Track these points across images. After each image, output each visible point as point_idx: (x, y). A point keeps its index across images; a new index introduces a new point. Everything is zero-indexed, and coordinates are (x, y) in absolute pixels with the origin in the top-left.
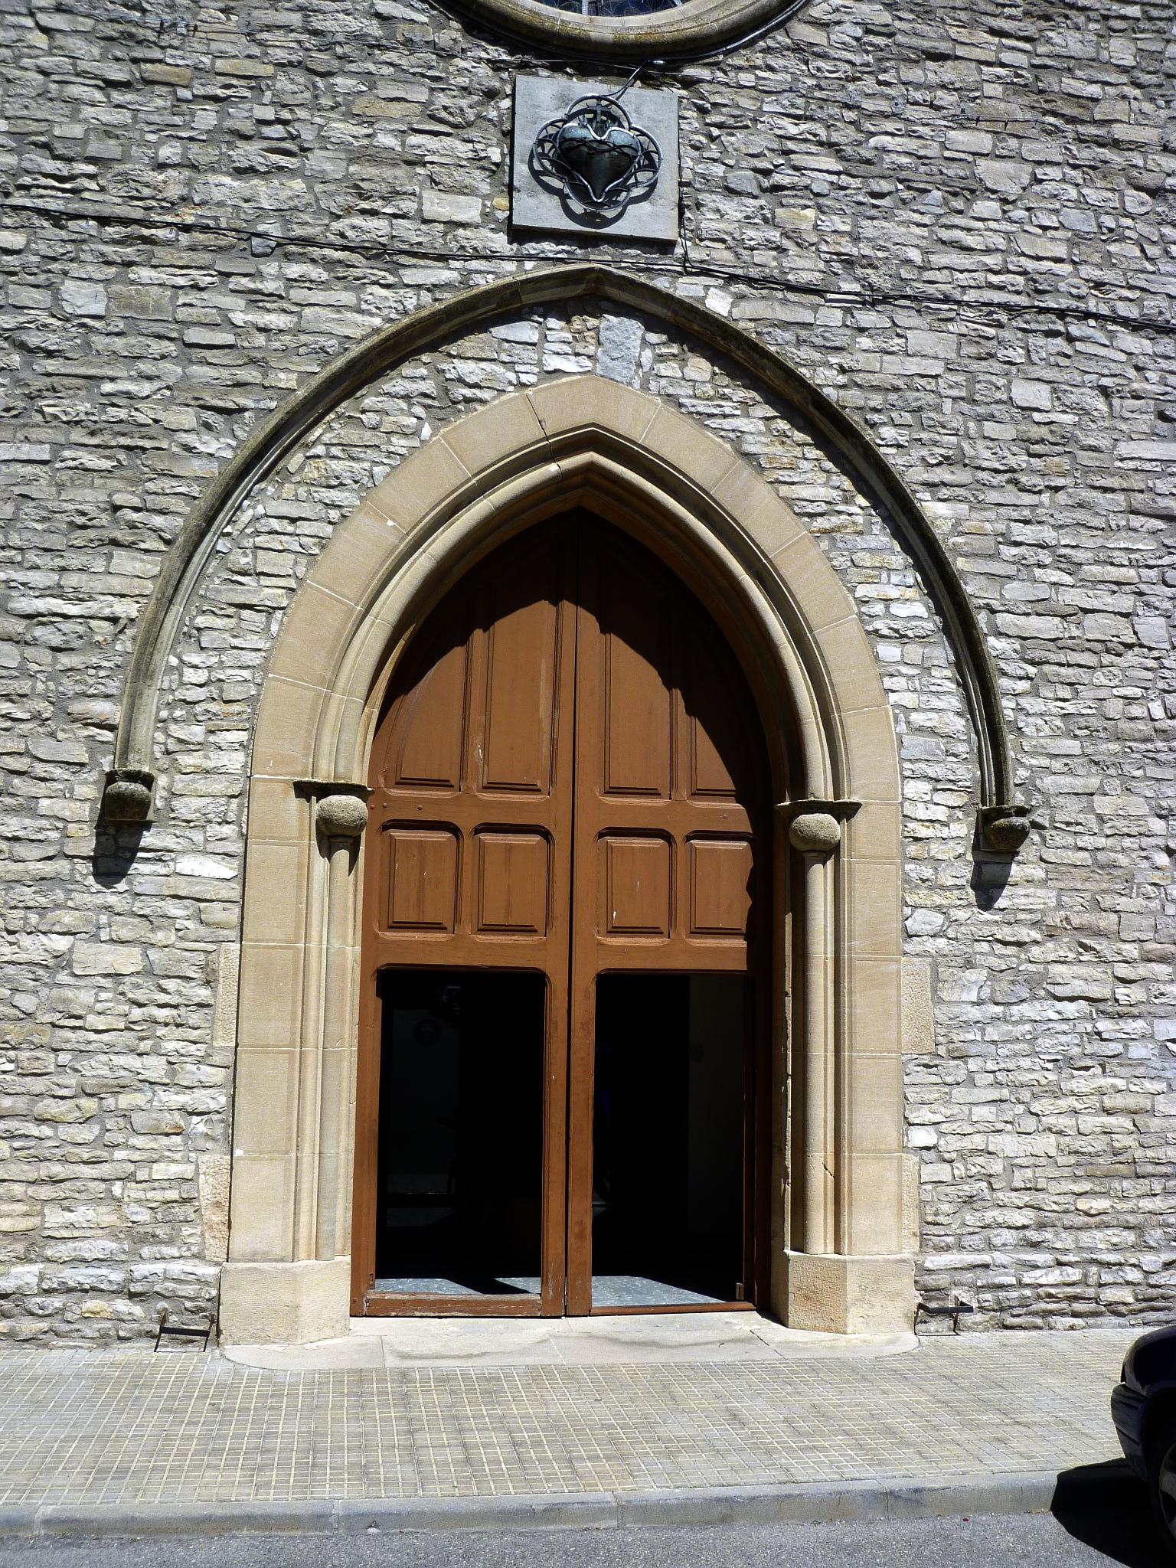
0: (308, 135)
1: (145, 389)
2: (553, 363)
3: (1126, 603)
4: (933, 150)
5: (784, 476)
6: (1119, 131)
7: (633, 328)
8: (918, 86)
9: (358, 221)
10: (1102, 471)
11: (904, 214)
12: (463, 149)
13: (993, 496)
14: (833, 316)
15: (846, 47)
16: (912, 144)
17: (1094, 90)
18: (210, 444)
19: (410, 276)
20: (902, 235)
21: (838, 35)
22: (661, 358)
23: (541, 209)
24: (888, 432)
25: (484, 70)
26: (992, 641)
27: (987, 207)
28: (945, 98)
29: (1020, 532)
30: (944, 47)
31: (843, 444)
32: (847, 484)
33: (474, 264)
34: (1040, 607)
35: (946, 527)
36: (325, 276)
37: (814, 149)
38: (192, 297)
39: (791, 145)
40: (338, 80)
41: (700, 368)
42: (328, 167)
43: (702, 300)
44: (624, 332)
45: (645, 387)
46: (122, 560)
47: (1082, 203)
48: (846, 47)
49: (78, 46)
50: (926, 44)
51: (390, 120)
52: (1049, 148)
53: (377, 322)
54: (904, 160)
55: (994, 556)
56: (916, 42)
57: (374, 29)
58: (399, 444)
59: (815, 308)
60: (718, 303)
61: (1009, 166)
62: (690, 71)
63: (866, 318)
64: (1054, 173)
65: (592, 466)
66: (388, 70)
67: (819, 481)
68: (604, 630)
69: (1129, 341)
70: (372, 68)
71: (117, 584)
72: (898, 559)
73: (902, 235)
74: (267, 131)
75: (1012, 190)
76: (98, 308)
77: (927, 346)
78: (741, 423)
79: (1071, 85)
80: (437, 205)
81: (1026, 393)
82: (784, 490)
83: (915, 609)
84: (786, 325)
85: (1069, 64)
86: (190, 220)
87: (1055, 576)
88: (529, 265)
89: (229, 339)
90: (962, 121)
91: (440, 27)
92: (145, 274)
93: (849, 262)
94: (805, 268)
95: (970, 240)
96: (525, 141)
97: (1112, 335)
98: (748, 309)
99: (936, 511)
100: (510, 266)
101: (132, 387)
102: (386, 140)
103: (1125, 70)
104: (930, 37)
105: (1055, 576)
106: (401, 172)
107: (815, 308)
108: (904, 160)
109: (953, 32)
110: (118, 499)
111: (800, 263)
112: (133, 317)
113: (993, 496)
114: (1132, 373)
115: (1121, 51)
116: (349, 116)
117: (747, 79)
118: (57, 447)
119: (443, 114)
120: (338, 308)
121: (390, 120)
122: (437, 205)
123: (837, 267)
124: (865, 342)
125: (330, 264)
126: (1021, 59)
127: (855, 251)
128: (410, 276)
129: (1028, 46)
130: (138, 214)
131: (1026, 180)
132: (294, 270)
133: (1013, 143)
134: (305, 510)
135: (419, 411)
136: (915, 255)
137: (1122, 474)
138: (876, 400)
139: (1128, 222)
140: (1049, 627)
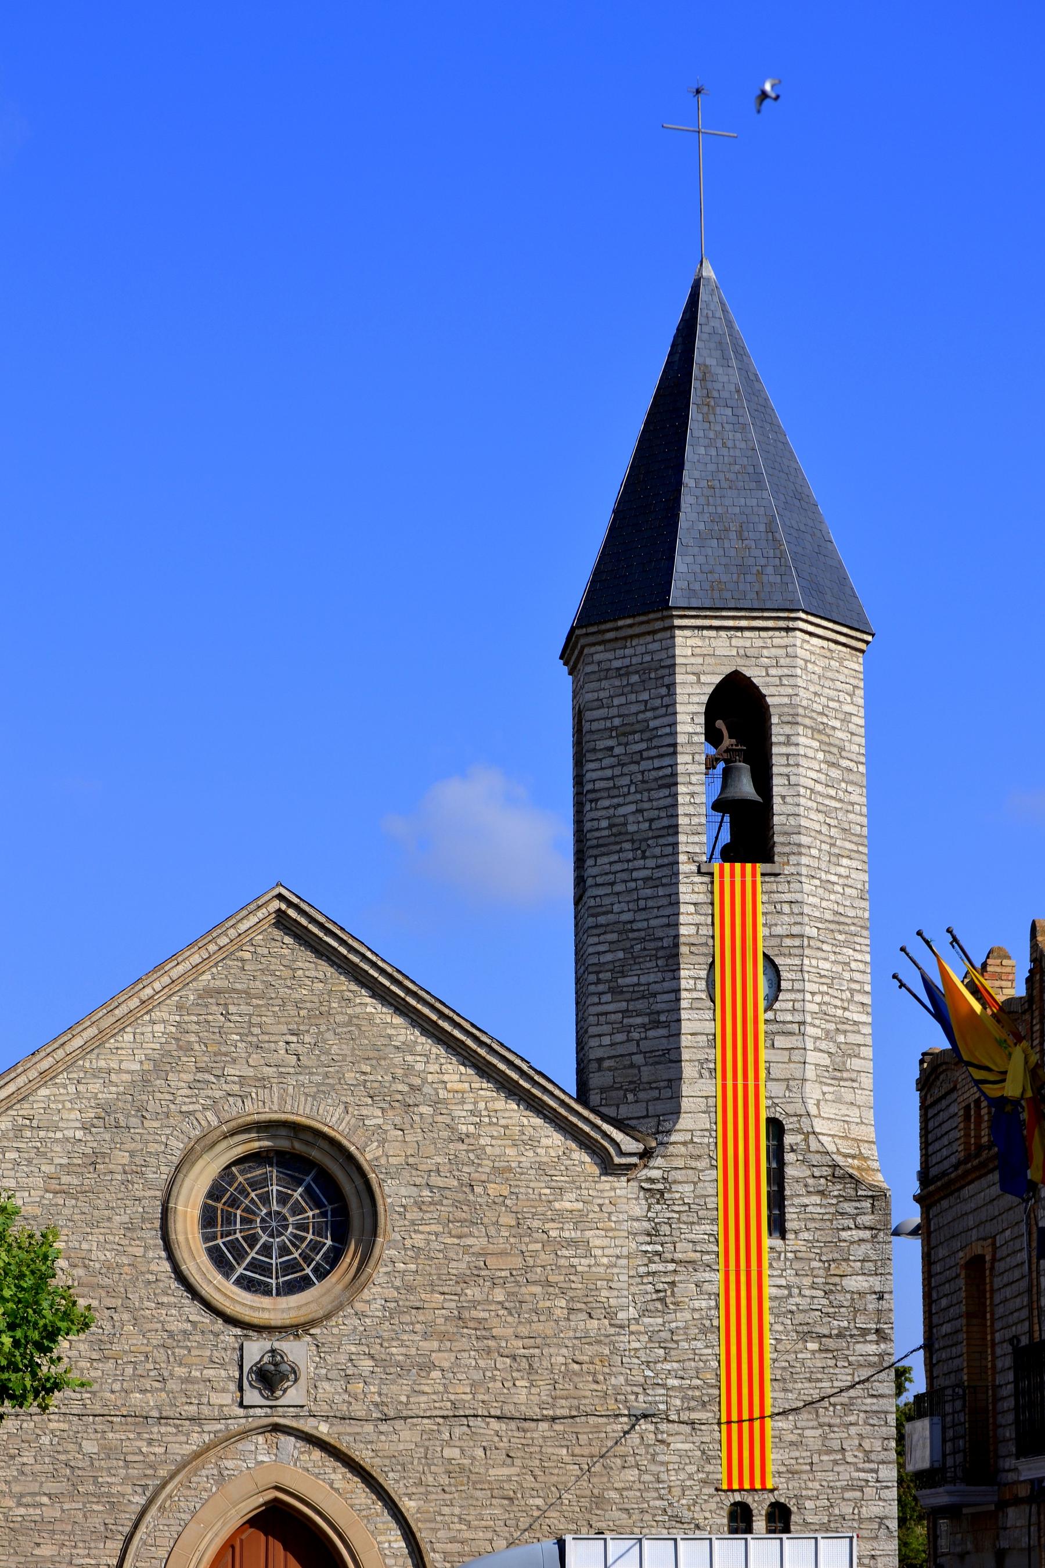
0: (166, 1374)
1: (115, 1483)
2: (260, 1458)
3: (489, 1535)
4: (413, 1351)
5: (348, 1496)
6: (495, 1332)
7: (293, 1439)
8: (407, 1324)
9: (186, 1407)
10: (481, 1482)
11: (401, 1381)
12: (223, 1373)
13: (434, 1497)
14: (369, 1428)
15: (377, 1310)
16: (403, 1350)
17: (486, 1315)
18: (136, 1499)
19: (206, 1428)
20: (399, 1391)
21: (373, 1306)
22: (302, 1453)
23: (252, 1396)
24: (391, 1475)
25: (232, 1339)
26: (432, 1554)
27: (436, 1374)
28: (418, 1327)
29: (446, 1510)
30: (418, 1304)
31: (373, 1482)
32: (374, 1497)
33: (229, 1421)
34: (452, 1540)
35: (414, 1511)
36: (174, 1431)
37: (362, 1357)
38: (128, 1443)
39: (353, 1357)
40: (177, 1350)
41: (317, 1454)
42: (174, 1386)
43: (317, 1428)
44: (289, 1442)
45: (295, 1465)
46: (110, 1544)
47: (477, 1367)
48: (377, 1310)
49: (82, 1347)
50: (411, 1304)
51: (196, 1365)
52: (464, 1343)
53: (195, 1448)
54: (401, 1358)
55: (435, 1521)
56: (407, 1303)
57: (188, 1327)
58: (205, 1495)
59: (362, 1426)
60: (323, 1429)
61: (446, 1355)
62: (312, 1331)
63: (383, 1427)
64: (465, 1355)
65: (276, 1500)
66: (194, 1344)
67: (363, 1496)
68: (285, 1549)
69: (494, 1424)
70: (189, 1344)
71: (108, 1552)
72: (393, 1525)
73: (399, 1391)
74: (152, 1373)
75: (446, 1365)
76: (95, 1450)
77: (407, 1436)
78: (333, 1476)
79: (474, 1313)
80: (216, 1399)
81: (448, 1453)
82: (349, 1501)
83: (400, 1544)
84: (349, 1434)
85: (475, 1304)
86: (125, 1413)
87: (458, 1526)
88: (250, 1419)
89: (141, 1458)
90: (426, 1337)
91: (213, 1323)
92: (110, 1435)
93: (376, 1405)
94: (359, 1410)
95: (426, 1389)
96: (246, 1370)
97: (488, 1424)
98: (335, 1429)
99: (409, 1506)
100: (243, 1421)
101: (109, 1480)
102: (196, 1373)
103: (499, 1303)
104: (413, 1300)
105: (458, 1526)
106: (201, 1386)
107: (362, 1426)
108: (401, 1358)
109: (423, 1296)
110: (107, 1521)
111: (356, 1408)
112: (108, 1451)
113: (434, 1497)
114: (496, 1439)
115: (499, 1295)
116: (180, 1365)
117: (335, 1331)
118: (84, 1504)
119: (217, 1360)
120: (181, 1443)
121: (196, 1365)
122: (216, 1399)
123: (372, 1407)
124: (383, 1438)
125: (176, 1426)
126: (453, 1305)
127: (379, 1400)
128: (206, 1428)
129: (456, 1298)
130: (106, 1412)
131: (453, 1359)
132: (163, 1429)
133: (448, 1344)
134: (172, 1522)
135: (212, 1481)
136: (404, 1399)
137: (490, 1482)
138: (387, 1462)
139: (498, 1373)
140: (455, 1547)
